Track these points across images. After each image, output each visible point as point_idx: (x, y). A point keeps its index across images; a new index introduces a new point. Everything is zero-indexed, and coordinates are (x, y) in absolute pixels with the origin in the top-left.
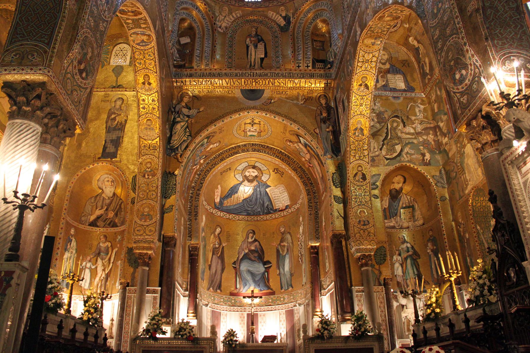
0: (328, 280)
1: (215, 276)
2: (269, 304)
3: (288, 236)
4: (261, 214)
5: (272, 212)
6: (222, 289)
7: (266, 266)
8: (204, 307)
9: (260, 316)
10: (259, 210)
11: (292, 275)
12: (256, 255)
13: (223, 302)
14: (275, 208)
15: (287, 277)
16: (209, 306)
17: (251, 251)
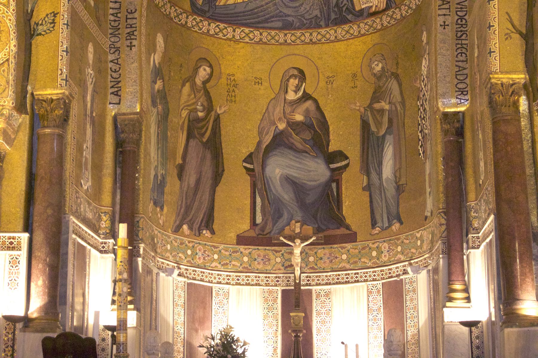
0: (483, 208)
1: (195, 194)
2: (341, 265)
3: (394, 85)
4: (322, 23)
5: (350, 17)
6: (215, 227)
7: (333, 166)
8: (162, 275)
9: (318, 295)
10: (317, 12)
11: (399, 189)
12: (307, 135)
13: (219, 261)
14: (357, 8)
15: (389, 195)
16: (176, 272)
17: (292, 125)
